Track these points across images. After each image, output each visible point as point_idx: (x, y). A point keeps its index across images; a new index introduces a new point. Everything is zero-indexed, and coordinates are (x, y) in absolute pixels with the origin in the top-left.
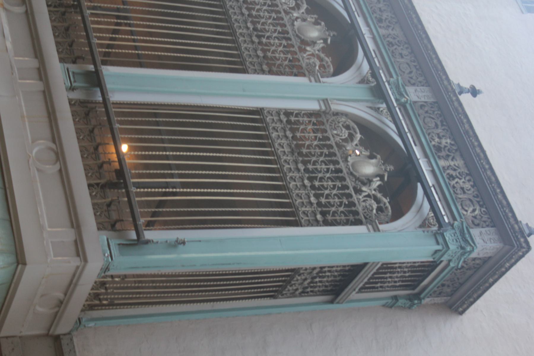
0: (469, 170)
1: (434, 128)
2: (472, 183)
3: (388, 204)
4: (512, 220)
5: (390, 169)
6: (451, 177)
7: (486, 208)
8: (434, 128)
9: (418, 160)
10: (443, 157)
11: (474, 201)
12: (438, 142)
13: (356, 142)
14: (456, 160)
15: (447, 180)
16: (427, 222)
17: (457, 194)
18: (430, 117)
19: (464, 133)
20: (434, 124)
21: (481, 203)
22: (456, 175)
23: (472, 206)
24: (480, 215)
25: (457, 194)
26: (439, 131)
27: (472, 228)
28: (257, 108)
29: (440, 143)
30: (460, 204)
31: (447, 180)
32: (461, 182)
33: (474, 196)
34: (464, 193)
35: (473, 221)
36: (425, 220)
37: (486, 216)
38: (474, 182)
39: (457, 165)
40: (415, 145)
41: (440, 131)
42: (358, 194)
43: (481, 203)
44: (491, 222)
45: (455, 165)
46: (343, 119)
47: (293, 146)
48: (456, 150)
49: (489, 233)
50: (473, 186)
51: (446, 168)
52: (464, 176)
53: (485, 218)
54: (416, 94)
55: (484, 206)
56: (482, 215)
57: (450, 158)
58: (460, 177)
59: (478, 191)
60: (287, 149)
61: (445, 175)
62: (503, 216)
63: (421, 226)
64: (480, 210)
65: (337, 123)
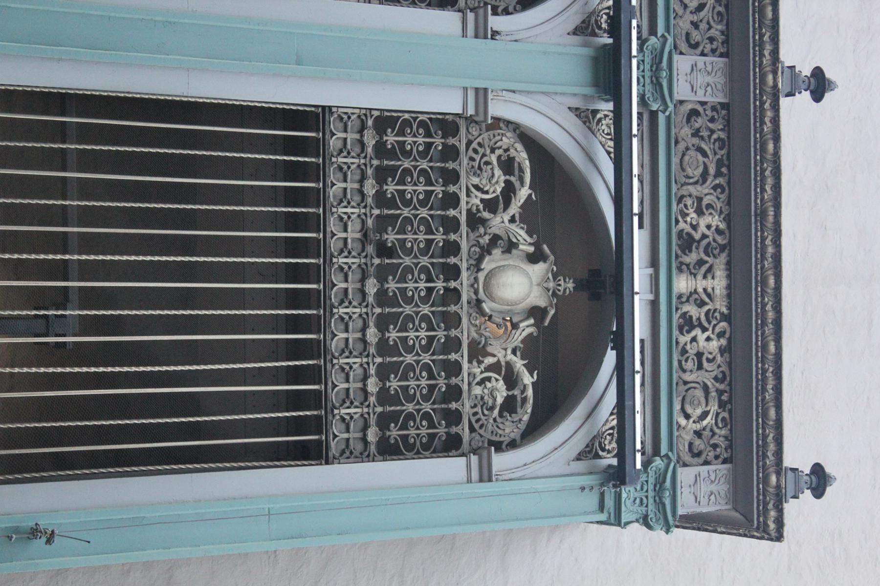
0: (729, 308)
1: (696, 183)
2: (723, 341)
3: (530, 392)
4: (768, 127)
5: (565, 290)
6: (688, 324)
7: (730, 412)
8: (696, 183)
9: (633, 293)
10: (688, 265)
11: (712, 389)
12: (691, 224)
13: (514, 209)
14: (713, 278)
15: (675, 332)
16: (593, 20)
17: (684, 371)
18: (700, 150)
19: (756, 215)
20: (701, 169)
21: (725, 397)
22: (699, 319)
23: (704, 405)
24: (708, 23)
25: (684, 371)
26: (705, 189)
27: (681, 53)
28: (316, 106)
29: (694, 227)
30: (680, 398)
31: (675, 332)
32: (702, 337)
33: (716, 379)
34: (700, 367)
35: (688, 35)
36: (589, 17)
37: (719, 27)
38: (729, 340)
39: (710, 290)
40: (641, 226)
41: (706, 191)
42: (475, 363)
43: (725, 397)
44: (723, 43)
45: (705, 290)
46: (506, 142)
47: (370, 222)
48: (723, 248)
49: (709, 68)
50: (722, 351)
51: (684, 299)
52: (714, 322)
53: (716, 31)
54: (696, 79)
55: (729, 406)
56: (712, 23)
57: (704, 268)
58: (706, 324)
59: (730, 364)
60: (353, 233)
61: (674, 231)
62: (758, 446)
63: (576, 32)
64: (714, 8)
65: (488, 151)
